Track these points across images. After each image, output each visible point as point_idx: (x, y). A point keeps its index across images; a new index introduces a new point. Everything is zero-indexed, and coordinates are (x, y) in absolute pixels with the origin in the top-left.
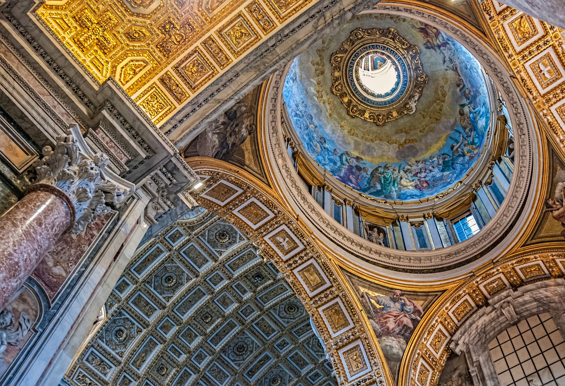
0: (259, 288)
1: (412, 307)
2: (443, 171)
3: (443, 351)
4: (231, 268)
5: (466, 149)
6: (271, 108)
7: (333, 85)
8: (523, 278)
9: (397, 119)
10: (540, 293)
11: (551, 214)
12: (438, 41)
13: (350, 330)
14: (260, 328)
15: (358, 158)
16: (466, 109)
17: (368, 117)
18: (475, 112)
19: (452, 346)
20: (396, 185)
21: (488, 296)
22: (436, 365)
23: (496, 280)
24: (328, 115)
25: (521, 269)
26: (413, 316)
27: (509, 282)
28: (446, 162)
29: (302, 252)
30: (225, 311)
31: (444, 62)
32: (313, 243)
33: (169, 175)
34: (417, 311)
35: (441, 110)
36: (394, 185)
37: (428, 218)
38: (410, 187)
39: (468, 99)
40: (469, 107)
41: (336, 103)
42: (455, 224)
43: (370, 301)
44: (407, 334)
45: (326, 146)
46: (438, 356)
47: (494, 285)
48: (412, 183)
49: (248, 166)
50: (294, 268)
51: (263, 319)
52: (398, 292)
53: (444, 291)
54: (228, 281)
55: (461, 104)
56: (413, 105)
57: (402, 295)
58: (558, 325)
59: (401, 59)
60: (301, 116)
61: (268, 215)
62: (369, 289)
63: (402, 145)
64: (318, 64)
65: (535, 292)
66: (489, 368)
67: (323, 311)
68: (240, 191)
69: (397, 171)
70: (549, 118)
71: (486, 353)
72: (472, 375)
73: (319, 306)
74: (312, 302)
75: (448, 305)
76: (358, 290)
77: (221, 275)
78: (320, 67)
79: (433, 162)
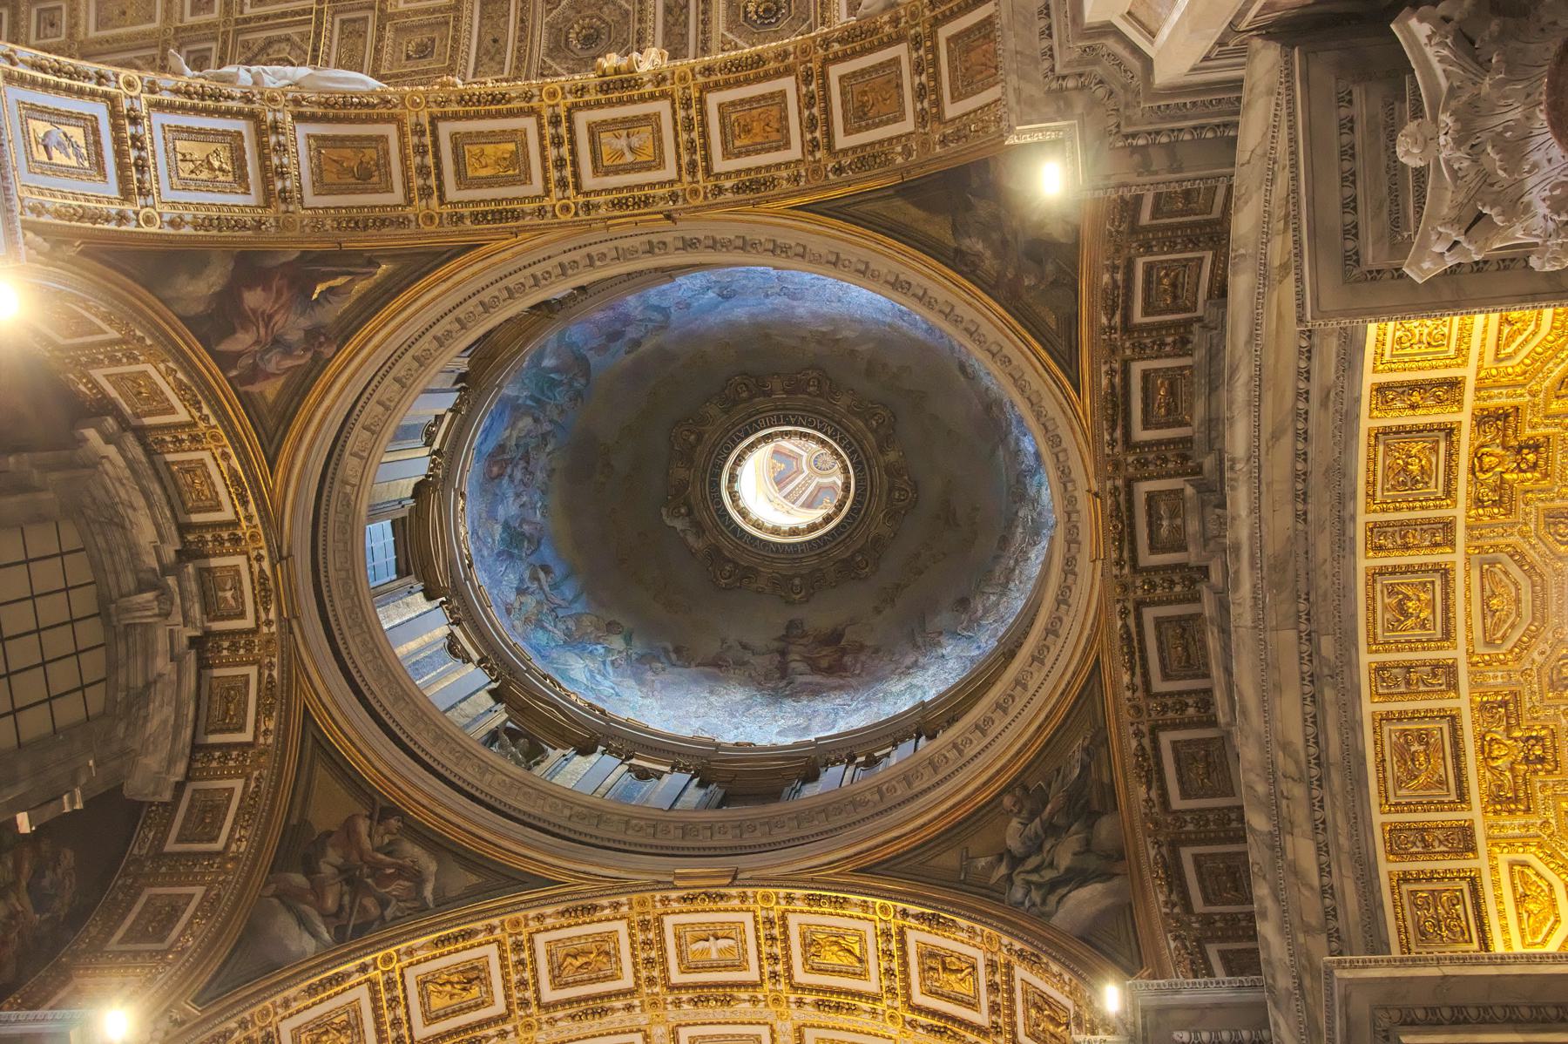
1: (271, 368)
3: (102, 391)
6: (958, 311)
8: (217, 672)
10: (162, 706)
18: (604, 663)
21: (202, 563)
23: (239, 597)
26: (246, 361)
29: (576, 174)
31: (745, 647)
33: (1141, 142)
34: (255, 374)
36: (532, 397)
37: (433, 461)
38: (507, 433)
40: (619, 652)
43: (349, 273)
45: (711, 294)
48: (514, 443)
49: (889, 197)
50: (541, 127)
56: (679, 524)
57: (316, 358)
62: (378, 286)
69: (556, 418)
70: (607, 911)
72: (11, 459)
74: (425, 121)
79: (534, 508)
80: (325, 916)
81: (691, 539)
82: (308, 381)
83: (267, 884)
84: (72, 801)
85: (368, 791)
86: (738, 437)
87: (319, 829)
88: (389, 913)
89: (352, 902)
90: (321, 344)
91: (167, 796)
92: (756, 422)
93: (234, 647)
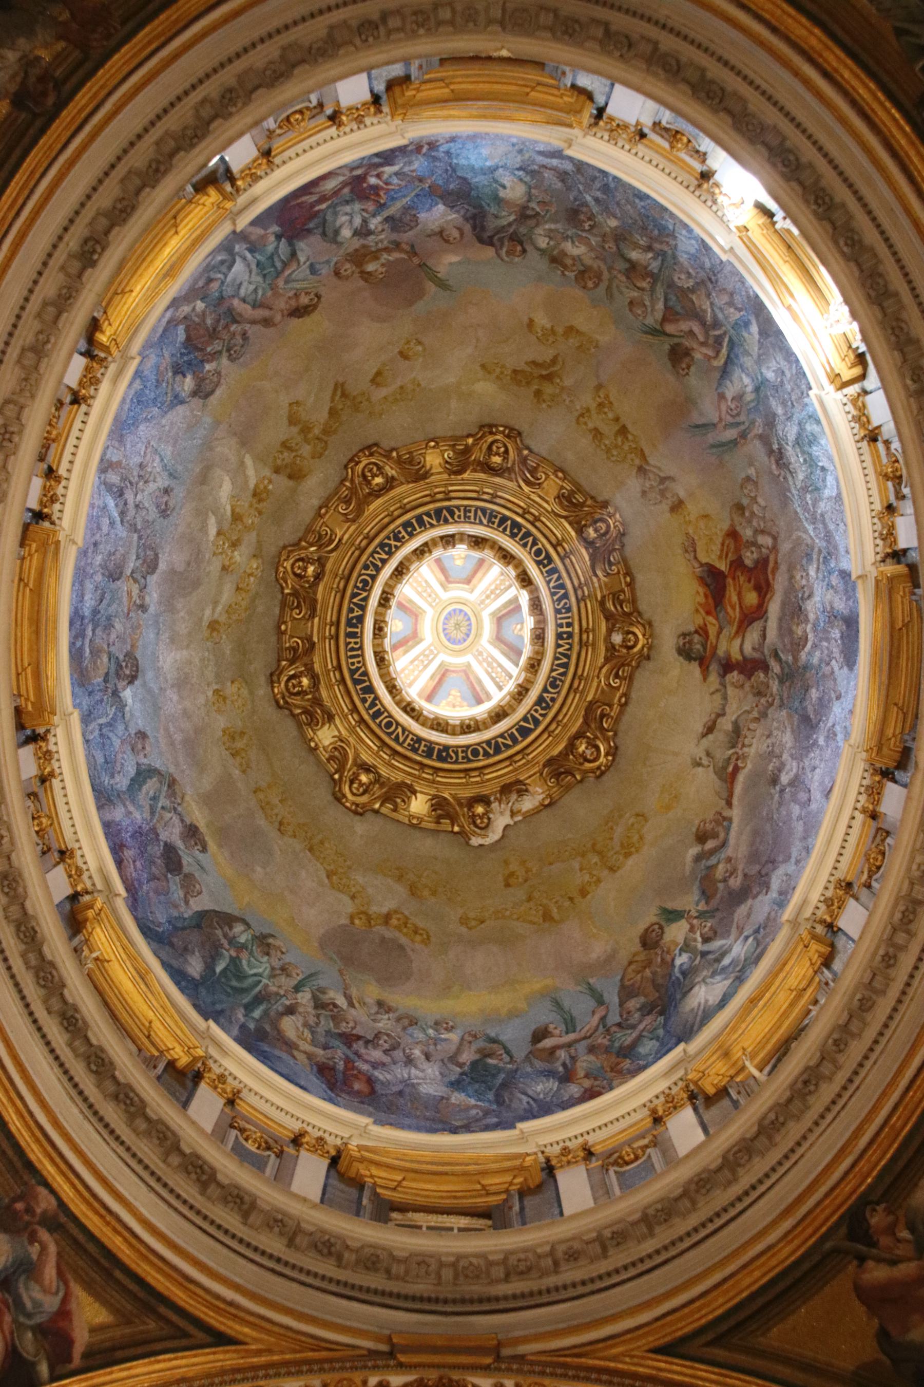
1: (51, 1303)
2: (456, 1085)
7: (297, 544)
11: (852, 1268)
12: (737, 642)
15: (192, 832)
16: (677, 932)
20: (257, 1014)
24: (205, 623)
28: (486, 1067)
31: (710, 729)
35: (583, 893)
36: (249, 1008)
38: (301, 1057)
40: (692, 929)
41: (260, 609)
45: (127, 694)
52: (45, 1202)
53: (221, 1339)
55: (670, 905)
56: (501, 821)
59: (570, 635)
63: (369, 918)
64: (305, 430)
69: (294, 982)
78: (306, 450)
81: (528, 804)
82: (91, 1247)
85: (816, 1258)
86: (373, 704)
87: (869, 1350)
90: (29, 1210)
92: (352, 672)
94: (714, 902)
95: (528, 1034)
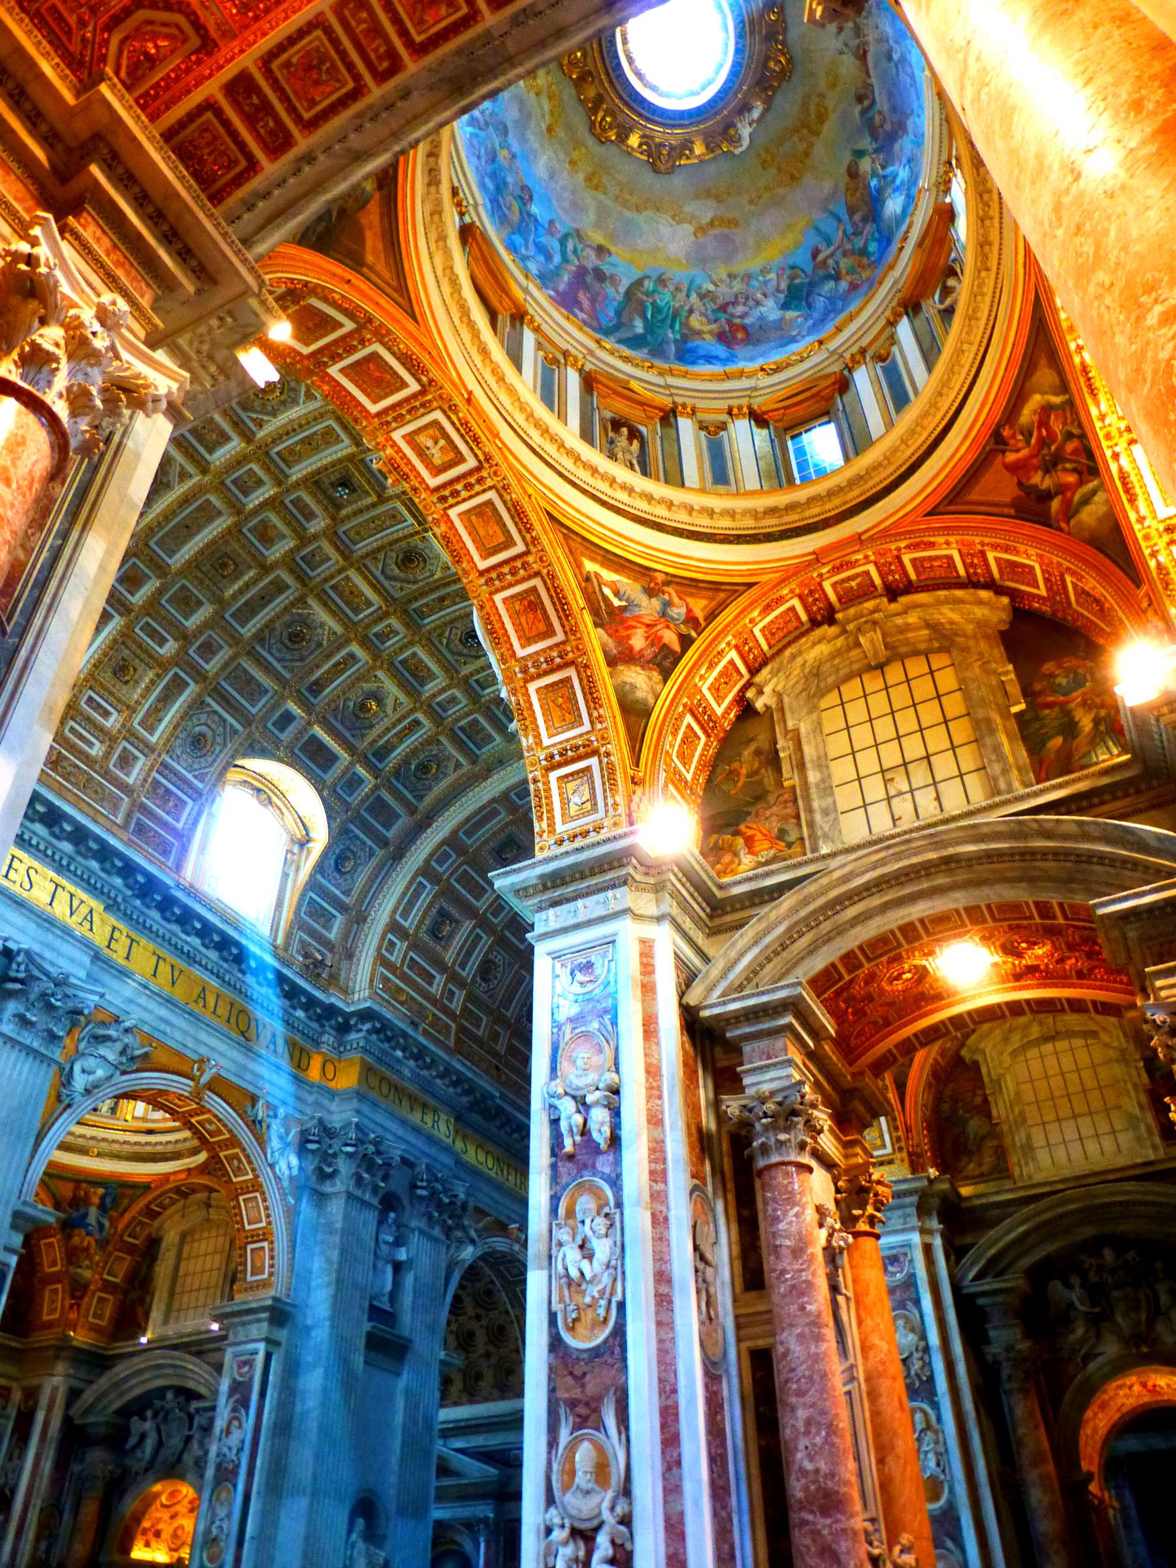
0: (344, 512)
1: (683, 610)
2: (785, 306)
4: (284, 460)
5: (845, 264)
8: (913, 576)
9: (701, 162)
13: (557, 645)
14: (341, 596)
15: (601, 250)
17: (636, 145)
18: (885, 177)
19: (750, 694)
20: (677, 327)
21: (836, 604)
22: (713, 728)
23: (858, 575)
25: (913, 561)
26: (683, 629)
27: (884, 582)
29: (470, 473)
30: (266, 553)
32: (497, 458)
34: (691, 620)
35: (807, 154)
36: (672, 327)
37: (737, 416)
38: (707, 336)
39: (874, 137)
40: (873, 161)
42: (792, 438)
44: (667, 663)
45: (534, 209)
46: (719, 711)
47: (853, 584)
49: (371, 268)
50: (451, 506)
51: (347, 578)
52: (660, 578)
54: (276, 490)
56: (745, 131)
57: (667, 583)
58: (961, 680)
60: (482, 123)
61: (404, 385)
62: (603, 564)
65: (930, 611)
66: (817, 746)
67: (505, 600)
68: (349, 326)
71: (814, 716)
72: (782, 755)
73: (497, 591)
74: (482, 580)
75: (756, 613)
76: (579, 566)
77: (261, 473)
80: (1081, 483)
81: (756, 114)
83: (1061, 530)
84: (1007, 673)
88: (1076, 431)
89: (1070, 461)
91: (1005, 600)
93: (892, 572)
94: (880, 141)
95: (809, 256)
